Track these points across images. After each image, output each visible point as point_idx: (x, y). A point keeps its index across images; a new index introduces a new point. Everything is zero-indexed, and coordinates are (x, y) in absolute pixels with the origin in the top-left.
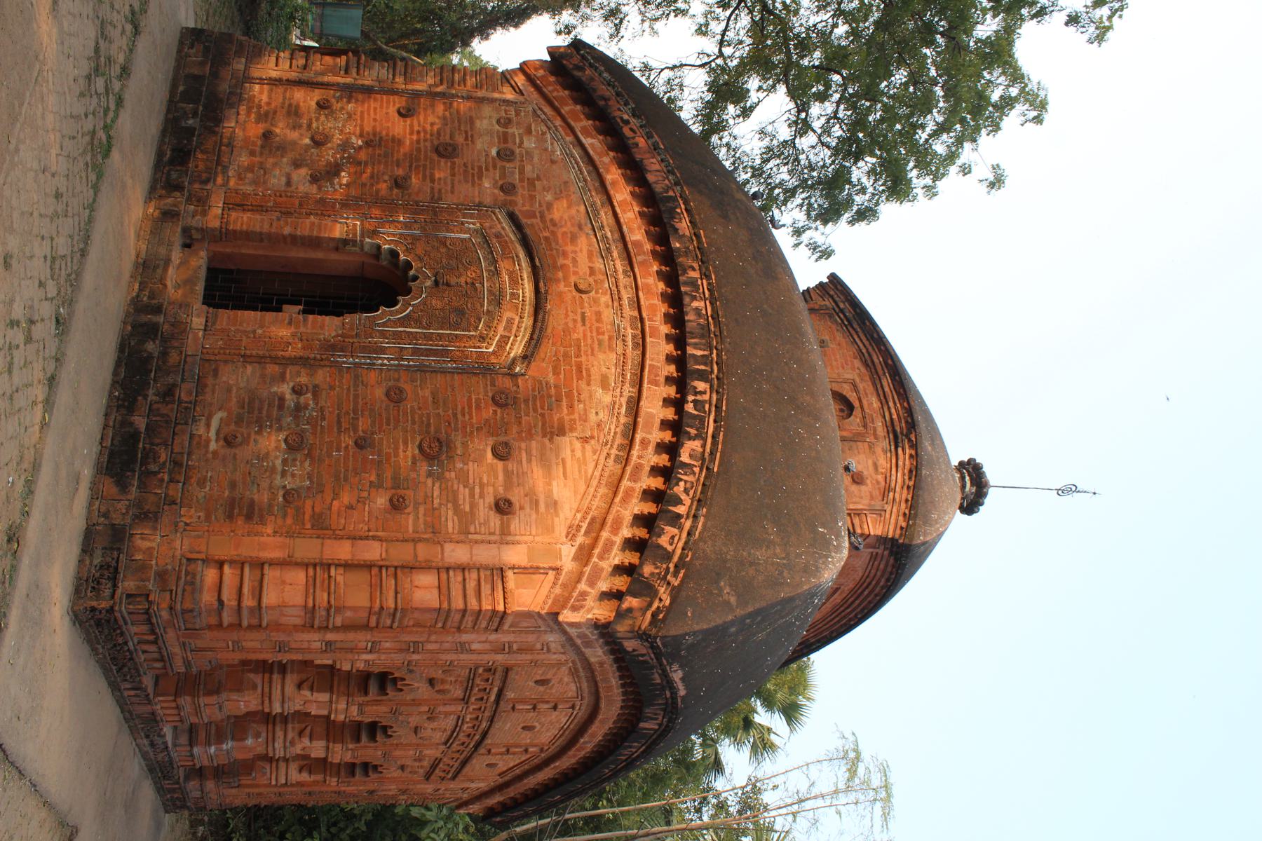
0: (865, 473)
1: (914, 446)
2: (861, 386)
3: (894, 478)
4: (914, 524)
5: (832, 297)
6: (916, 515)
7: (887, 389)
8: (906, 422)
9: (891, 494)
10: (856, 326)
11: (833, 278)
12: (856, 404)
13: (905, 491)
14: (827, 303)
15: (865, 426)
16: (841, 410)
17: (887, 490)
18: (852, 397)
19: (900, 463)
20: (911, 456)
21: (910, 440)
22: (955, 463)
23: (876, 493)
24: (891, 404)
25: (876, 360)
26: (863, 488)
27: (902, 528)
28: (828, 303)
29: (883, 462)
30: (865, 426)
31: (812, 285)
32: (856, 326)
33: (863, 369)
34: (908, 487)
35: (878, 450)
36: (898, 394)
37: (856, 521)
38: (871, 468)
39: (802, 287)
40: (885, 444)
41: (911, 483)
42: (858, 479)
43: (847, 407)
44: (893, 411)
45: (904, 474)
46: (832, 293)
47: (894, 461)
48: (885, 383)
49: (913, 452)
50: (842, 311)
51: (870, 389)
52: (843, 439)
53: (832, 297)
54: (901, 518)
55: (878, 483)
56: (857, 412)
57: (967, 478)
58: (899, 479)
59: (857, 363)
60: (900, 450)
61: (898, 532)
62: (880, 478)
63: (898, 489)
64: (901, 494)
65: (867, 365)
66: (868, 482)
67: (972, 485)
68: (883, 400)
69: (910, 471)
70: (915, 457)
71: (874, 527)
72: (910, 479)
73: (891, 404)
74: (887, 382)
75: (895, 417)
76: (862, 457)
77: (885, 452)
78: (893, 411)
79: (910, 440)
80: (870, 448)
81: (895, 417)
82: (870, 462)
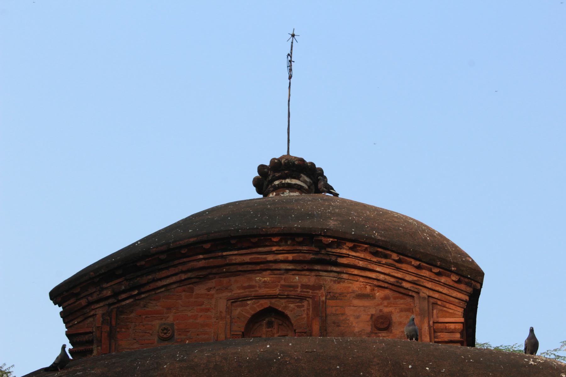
0: (373, 311)
1: (340, 240)
2: (237, 292)
3: (382, 277)
4: (456, 265)
5: (90, 304)
6: (442, 260)
7: (247, 259)
8: (300, 244)
9: (405, 284)
10: (144, 280)
11: (58, 295)
12: (266, 303)
13: (404, 266)
14: (100, 312)
15: (301, 298)
16: (270, 324)
17: (397, 287)
18: (253, 307)
19: (361, 264)
20: (352, 249)
21: (330, 245)
22: (253, 194)
23: (402, 302)
24: (270, 257)
25: (201, 264)
26: (396, 318)
27: (459, 282)
28: (99, 311)
29: (357, 286)
30: (301, 298)
31: (63, 328)
32: (144, 280)
33: (212, 283)
34: (399, 261)
35: (337, 288)
36: (256, 245)
37: (445, 336)
38: (366, 303)
39: (523, 348)
40: (328, 279)
41: (395, 256)
42: (382, 324)
43: (270, 317)
44: (281, 257)
45: (379, 264)
46: (83, 302)
47: (356, 272)
48: (239, 259)
49: (350, 245)
50: (116, 294)
51: (242, 280)
52: (324, 332)
53: (90, 304)
54: (443, 279)
55: (386, 298)
56: (280, 305)
57: (288, 181)
58: (383, 271)
59: (200, 289)
60: (341, 260)
61: (462, 287)
62: (379, 294)
63: (399, 275)
64: (407, 273)
65: (205, 278)
66: (386, 310)
67: (298, 178)
68: (262, 266)
69: (375, 254)
70: (357, 243)
71: (453, 315)
72: (386, 257)
73: (270, 257)
74: (236, 257)
75: (290, 257)
76: (349, 311)
77: (340, 280)
78: (281, 257)
79: (330, 245)
80: (334, 298)
81: (290, 257)
82: (356, 302)
